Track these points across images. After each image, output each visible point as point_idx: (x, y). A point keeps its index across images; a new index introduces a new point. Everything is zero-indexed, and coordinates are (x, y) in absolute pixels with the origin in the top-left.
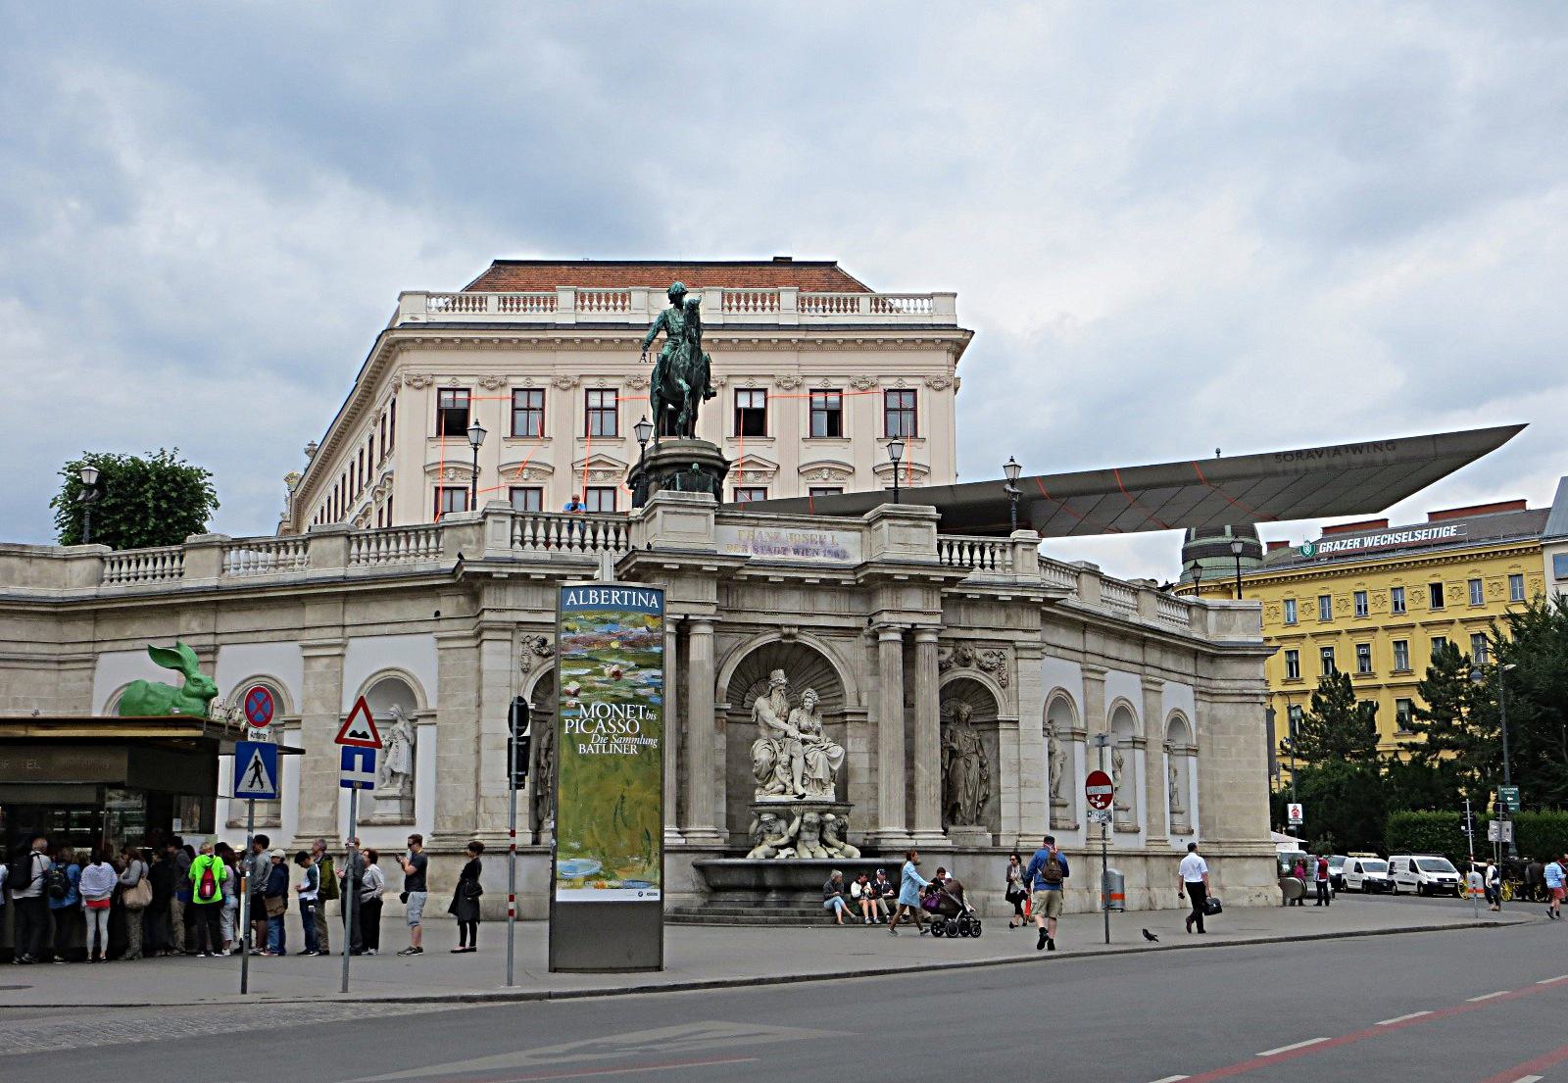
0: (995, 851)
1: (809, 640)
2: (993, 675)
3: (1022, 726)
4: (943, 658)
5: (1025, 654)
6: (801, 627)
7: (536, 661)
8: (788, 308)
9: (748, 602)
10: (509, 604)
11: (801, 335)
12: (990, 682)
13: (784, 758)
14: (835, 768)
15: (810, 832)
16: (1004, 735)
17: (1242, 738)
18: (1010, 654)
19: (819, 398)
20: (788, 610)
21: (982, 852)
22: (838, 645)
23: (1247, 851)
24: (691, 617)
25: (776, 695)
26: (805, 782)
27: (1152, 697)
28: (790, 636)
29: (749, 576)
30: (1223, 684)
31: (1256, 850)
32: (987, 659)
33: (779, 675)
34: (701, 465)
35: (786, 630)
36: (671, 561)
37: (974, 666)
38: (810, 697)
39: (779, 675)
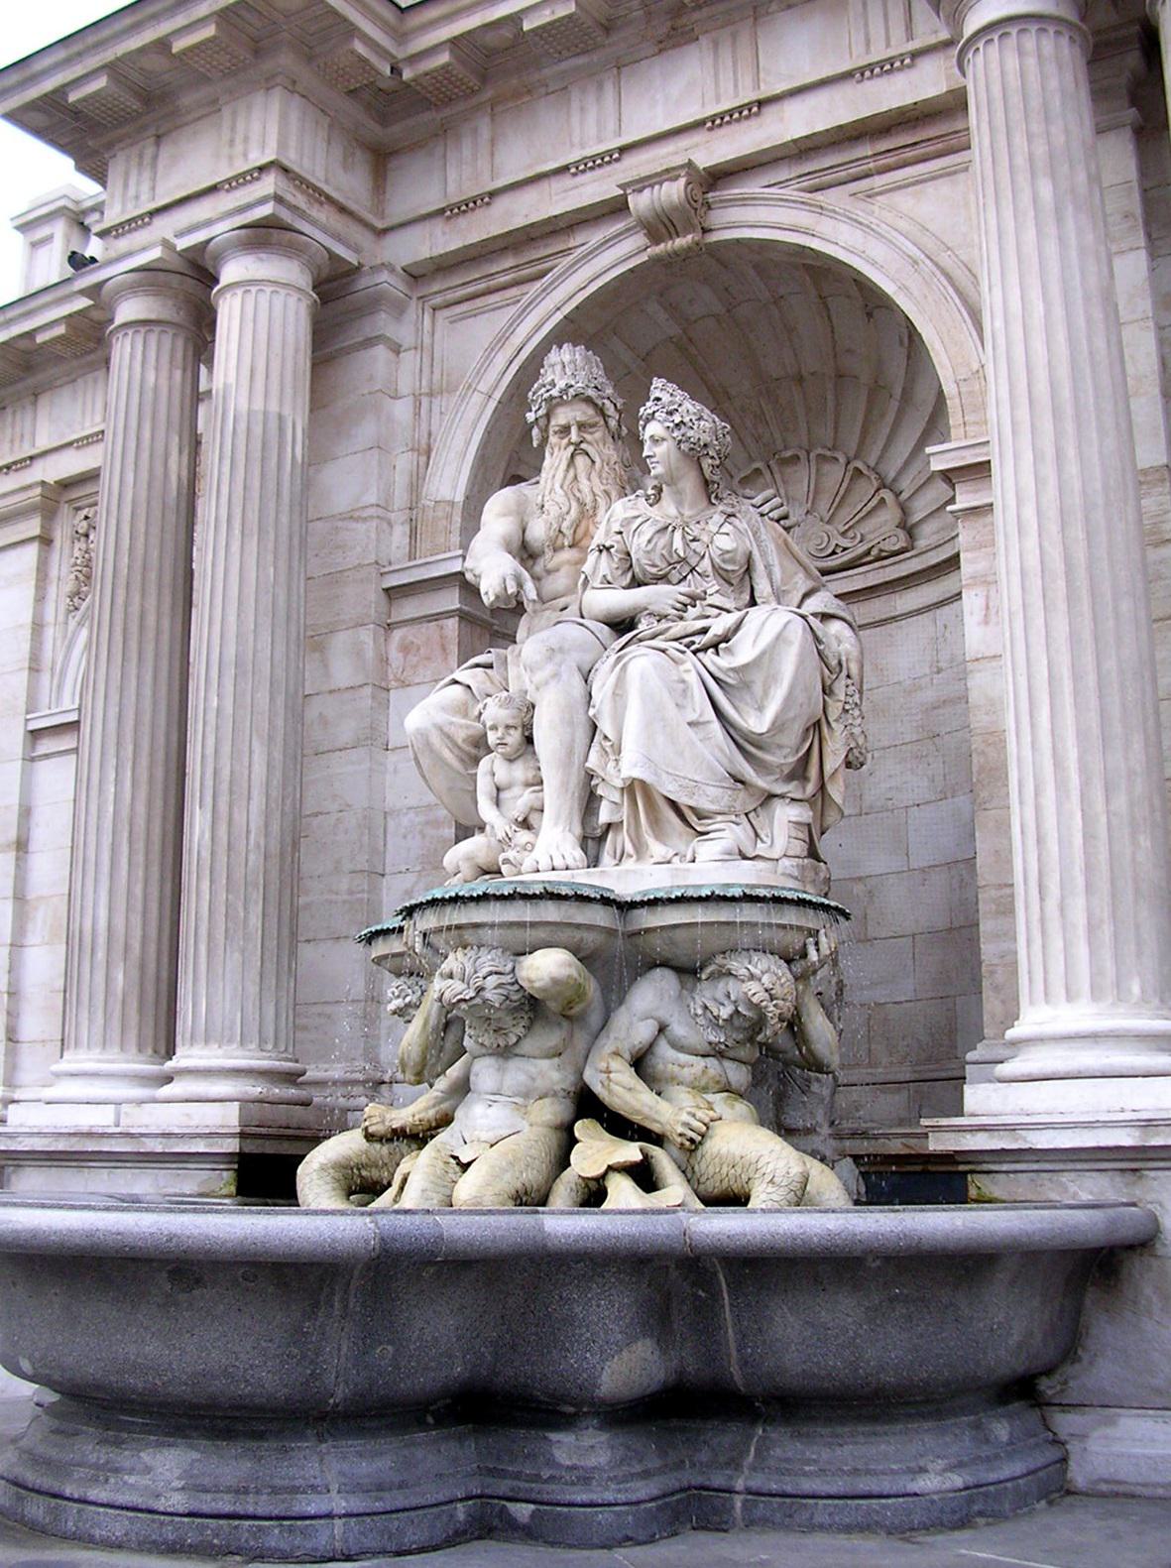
1: (762, 216)
9: (515, 162)
10: (43, 442)
13: (494, 712)
14: (757, 723)
15: (505, 1053)
22: (903, 200)
24: (182, 244)
25: (555, 461)
26: (604, 815)
28: (659, 226)
29: (454, 42)
33: (567, 369)
35: (640, 202)
36: (78, 70)
38: (671, 416)
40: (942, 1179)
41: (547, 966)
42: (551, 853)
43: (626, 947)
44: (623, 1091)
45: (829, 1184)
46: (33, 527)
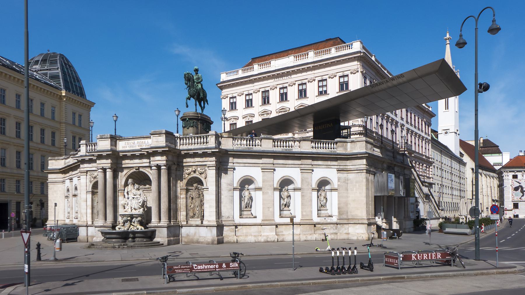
0: (202, 225)
2: (203, 175)
3: (209, 189)
4: (189, 171)
5: (210, 168)
6: (139, 167)
7: (92, 179)
8: (312, 56)
11: (313, 65)
12: (202, 178)
16: (205, 193)
17: (357, 184)
18: (207, 168)
19: (321, 84)
20: (136, 163)
21: (197, 226)
23: (357, 221)
25: (130, 186)
27: (305, 175)
28: (136, 169)
30: (351, 167)
31: (360, 222)
32: (201, 170)
34: (189, 119)
37: (197, 173)
38: (137, 186)
39: (130, 181)
40: (147, 228)
41: (129, 218)
42: (129, 212)
43: (132, 216)
44: (133, 223)
45: (143, 228)
46: (85, 174)
